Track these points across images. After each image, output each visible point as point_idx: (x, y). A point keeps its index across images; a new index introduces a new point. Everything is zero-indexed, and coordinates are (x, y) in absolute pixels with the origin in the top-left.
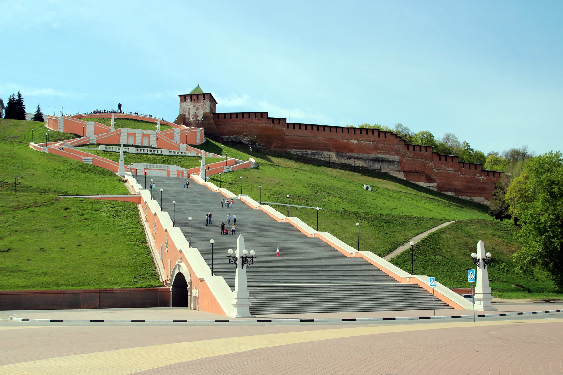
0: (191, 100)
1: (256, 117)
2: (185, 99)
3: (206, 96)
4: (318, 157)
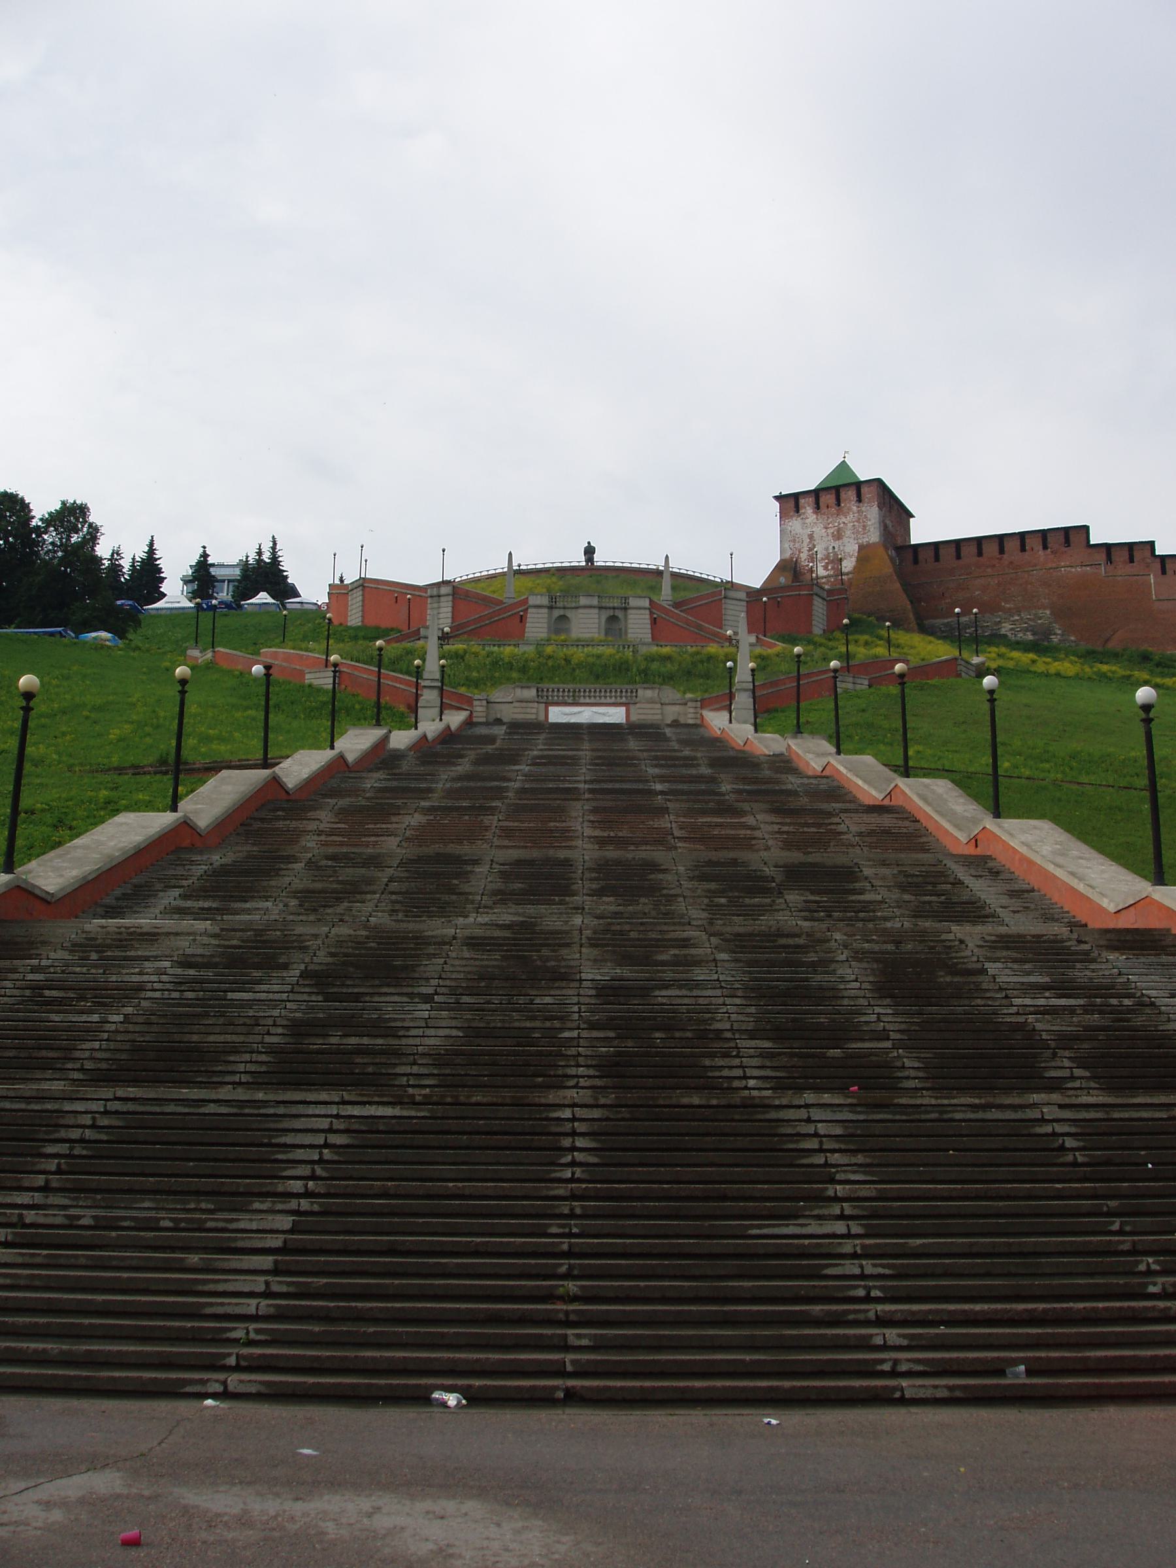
0: (817, 507)
1: (1045, 547)
3: (864, 489)
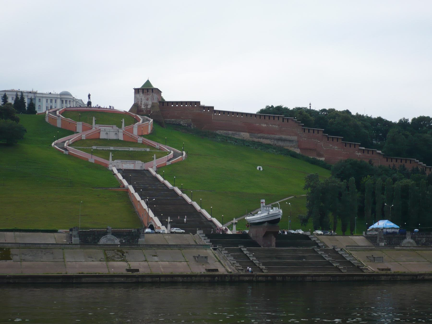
0: (143, 92)
2: (138, 92)
3: (154, 90)
4: (236, 137)
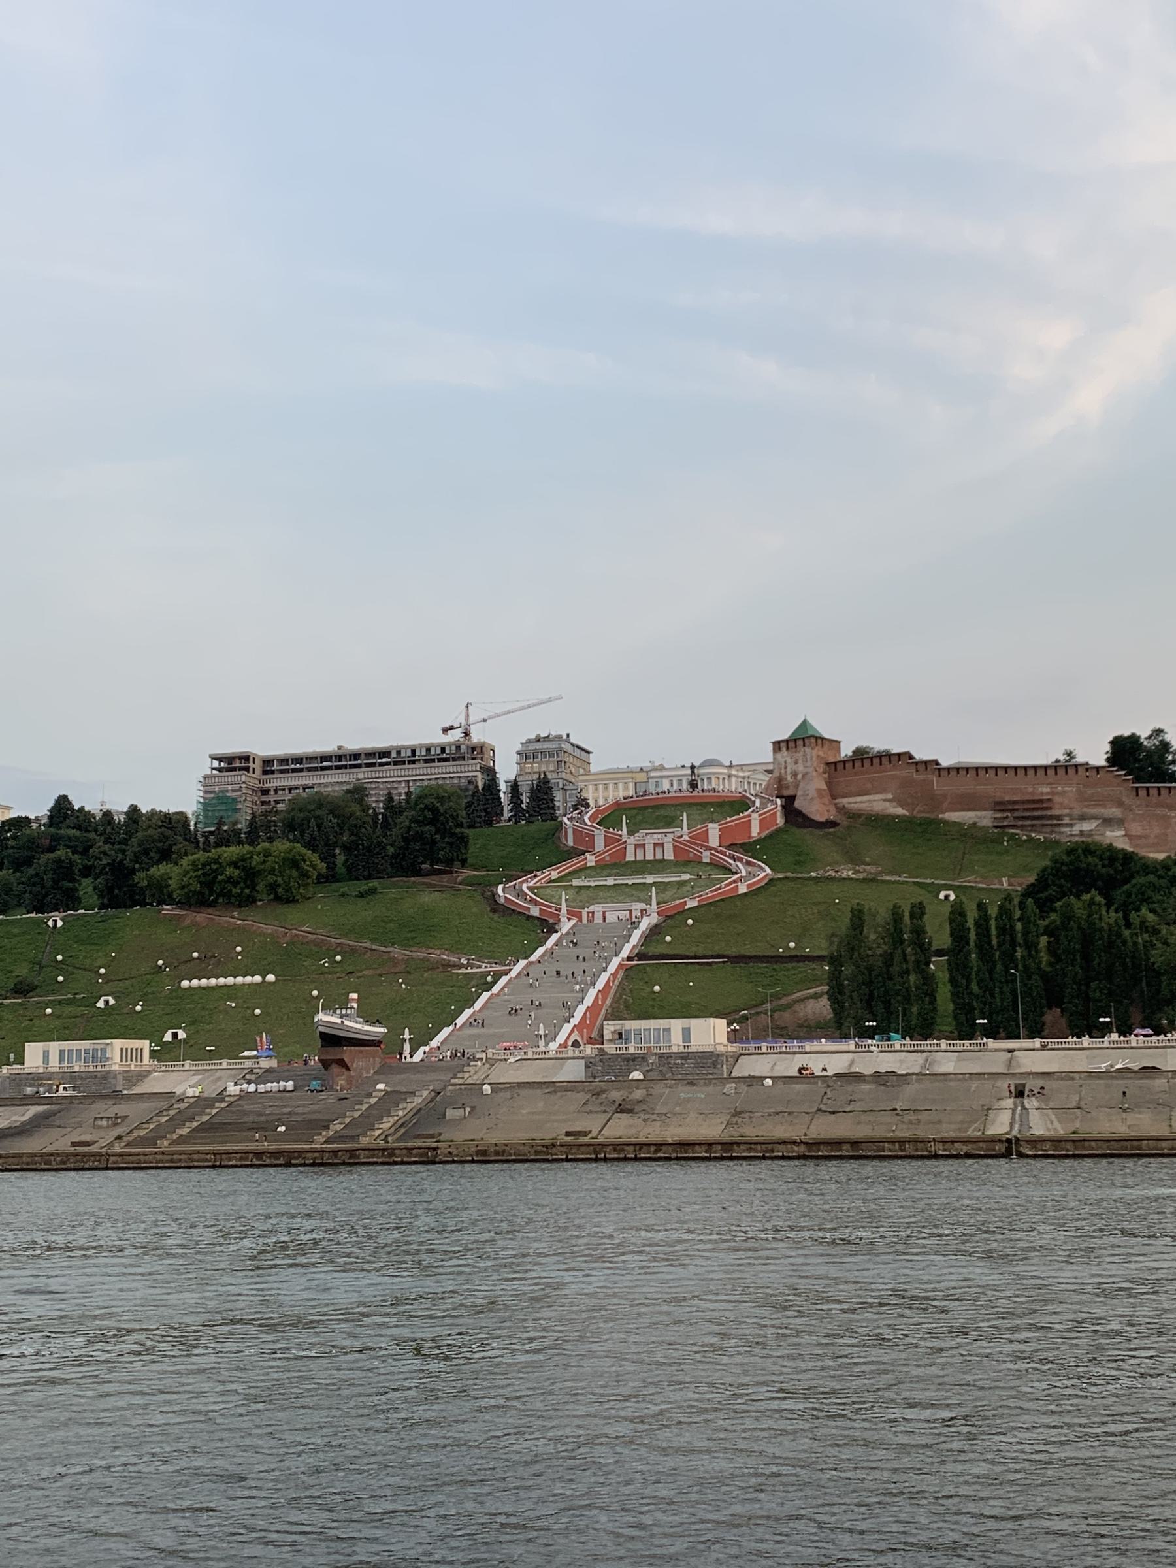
0: (788, 748)
2: (780, 749)
